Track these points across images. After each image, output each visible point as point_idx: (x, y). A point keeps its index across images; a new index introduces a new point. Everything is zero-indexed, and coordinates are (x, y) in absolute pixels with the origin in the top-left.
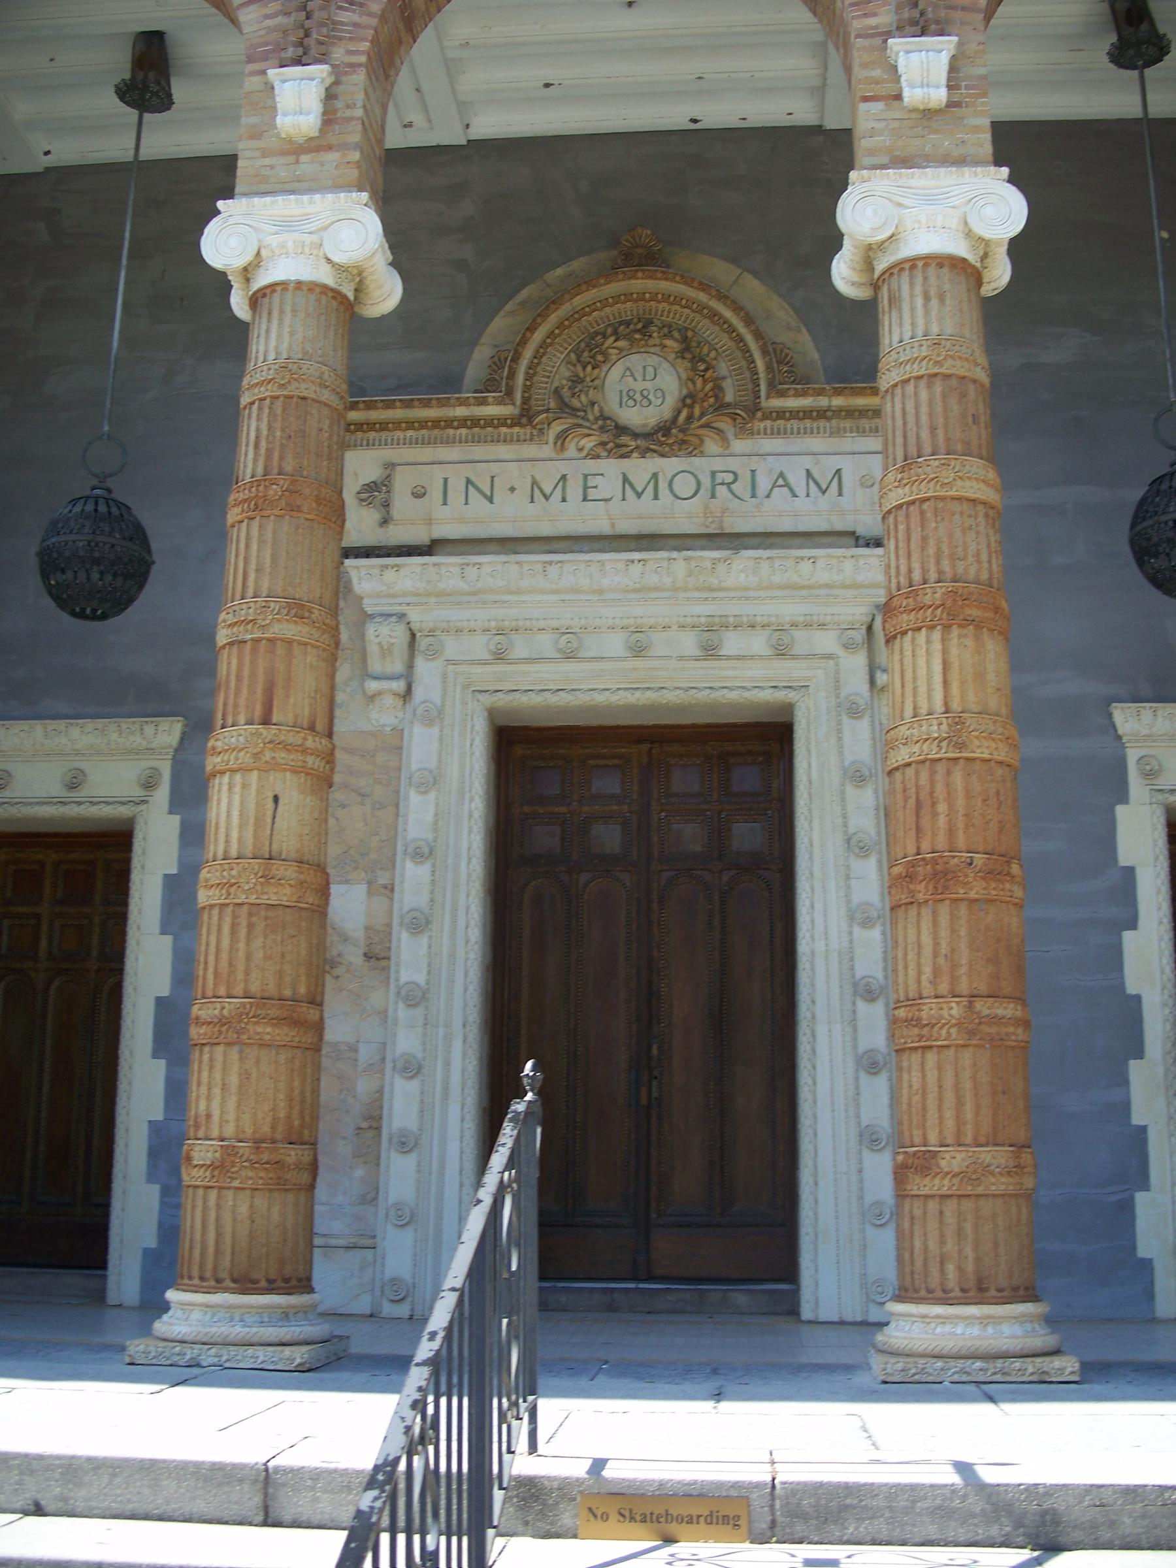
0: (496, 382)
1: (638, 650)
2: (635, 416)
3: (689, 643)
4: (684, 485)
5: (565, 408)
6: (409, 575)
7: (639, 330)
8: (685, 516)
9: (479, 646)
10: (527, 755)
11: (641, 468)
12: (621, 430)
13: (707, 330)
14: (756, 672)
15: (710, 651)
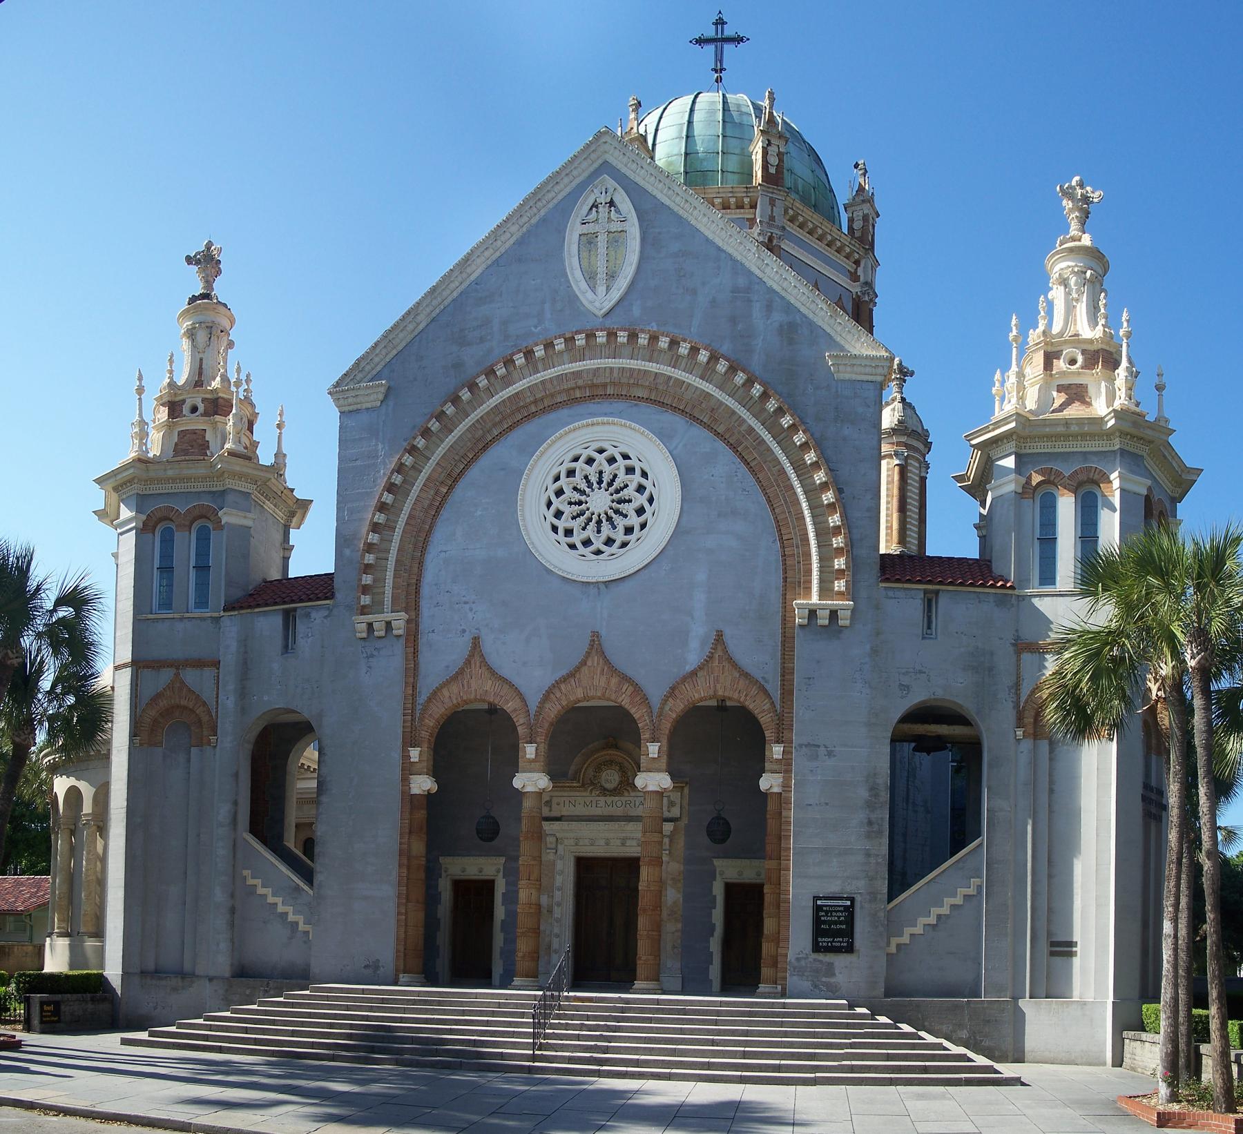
0: (575, 778)
1: (607, 844)
2: (608, 786)
3: (618, 842)
4: (619, 804)
5: (592, 783)
6: (556, 826)
7: (610, 763)
8: (619, 812)
9: (572, 842)
10: (584, 865)
11: (610, 799)
12: (605, 789)
13: (626, 764)
14: (633, 849)
15: (623, 844)
